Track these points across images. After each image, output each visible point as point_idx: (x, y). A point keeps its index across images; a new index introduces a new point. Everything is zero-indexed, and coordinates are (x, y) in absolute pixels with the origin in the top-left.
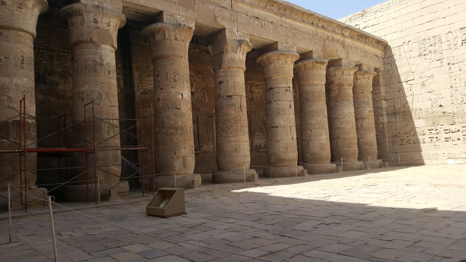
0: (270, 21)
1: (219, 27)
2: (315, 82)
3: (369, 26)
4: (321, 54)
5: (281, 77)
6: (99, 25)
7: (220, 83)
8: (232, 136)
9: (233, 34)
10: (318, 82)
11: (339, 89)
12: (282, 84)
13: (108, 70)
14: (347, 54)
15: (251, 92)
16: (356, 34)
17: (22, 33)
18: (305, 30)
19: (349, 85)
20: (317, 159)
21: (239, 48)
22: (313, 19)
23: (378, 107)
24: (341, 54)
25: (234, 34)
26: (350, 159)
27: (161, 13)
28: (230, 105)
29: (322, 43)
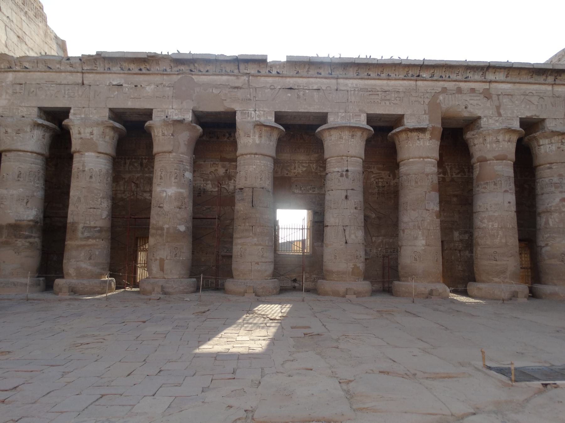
0: (315, 88)
11: (480, 166)
12: (335, 168)
13: (90, 175)
14: (498, 108)
17: (21, 153)
18: (386, 88)
26: (496, 279)
29: (427, 101)
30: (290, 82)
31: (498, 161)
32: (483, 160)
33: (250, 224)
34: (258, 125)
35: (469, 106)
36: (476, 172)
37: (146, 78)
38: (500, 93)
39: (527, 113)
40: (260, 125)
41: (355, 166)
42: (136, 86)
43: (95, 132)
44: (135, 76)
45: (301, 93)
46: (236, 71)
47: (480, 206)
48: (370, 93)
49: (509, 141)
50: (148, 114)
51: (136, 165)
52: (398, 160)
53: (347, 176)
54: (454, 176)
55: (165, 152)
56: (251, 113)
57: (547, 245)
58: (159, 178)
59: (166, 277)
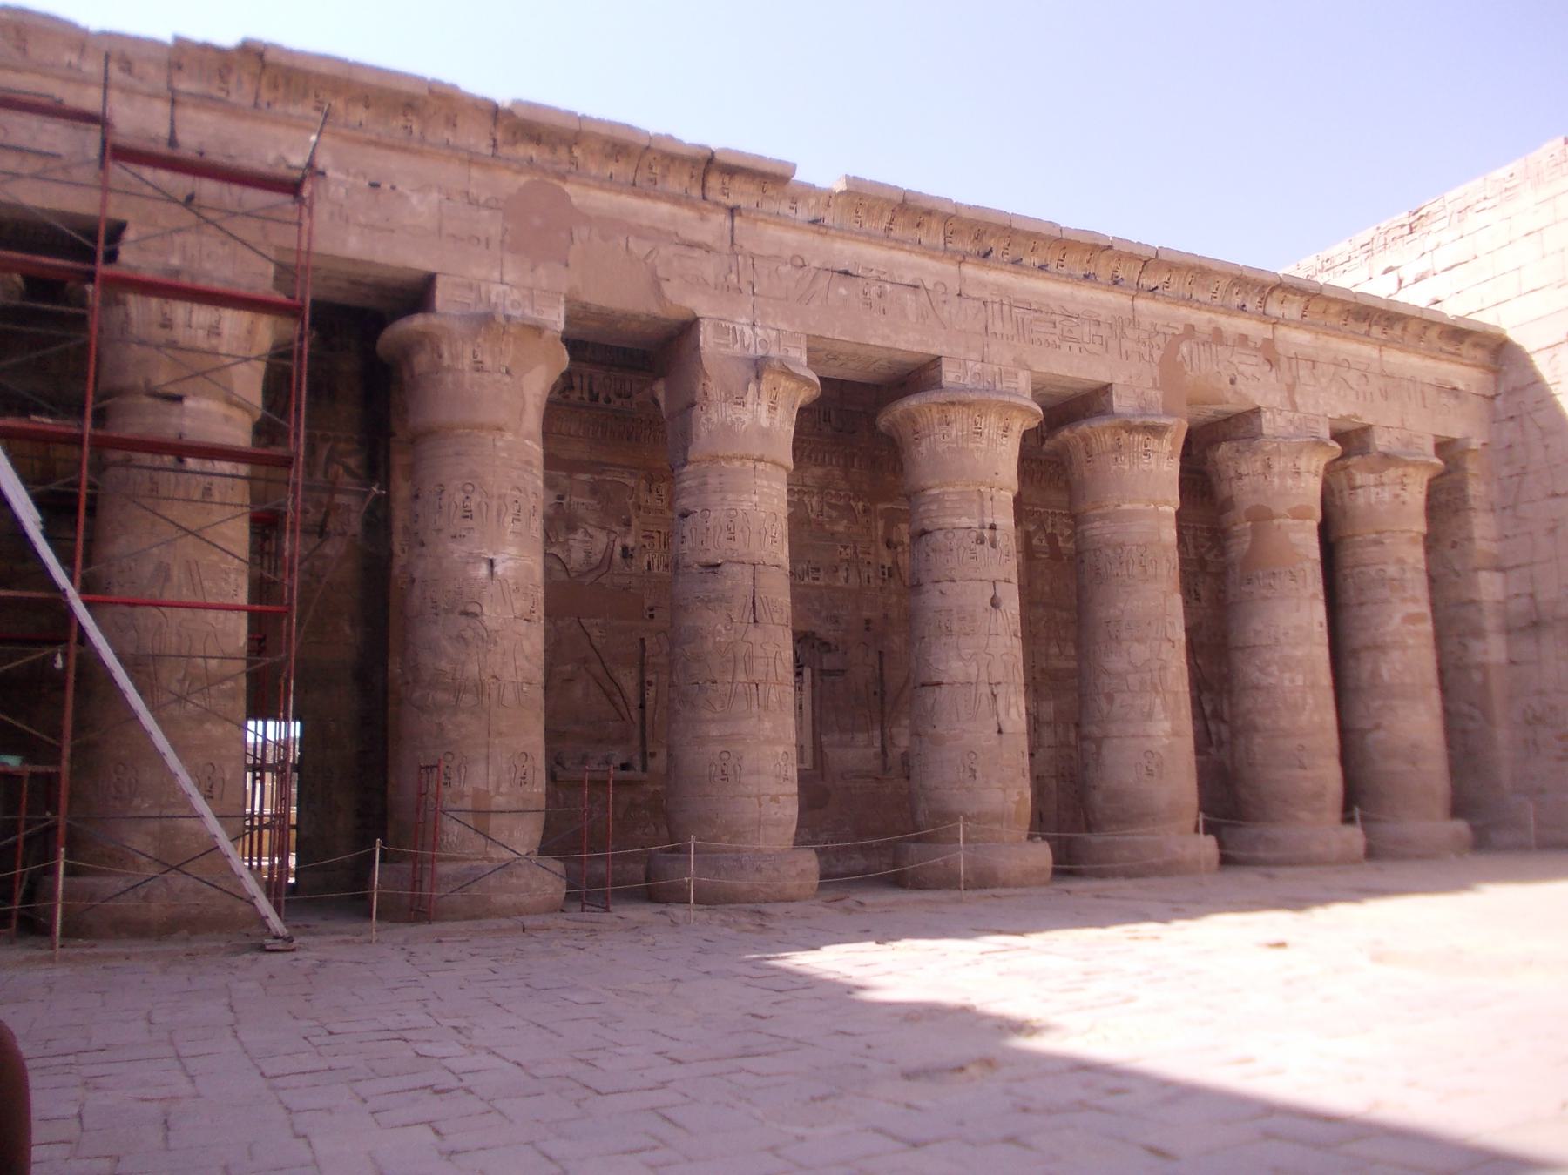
0: (907, 281)
1: (674, 315)
2: (1126, 507)
3: (1438, 269)
4: (1156, 396)
5: (958, 488)
6: (180, 334)
7: (684, 515)
8: (713, 720)
9: (730, 333)
10: (1140, 506)
12: (960, 516)
15: (889, 544)
16: (1334, 309)
18: (1071, 308)
19: (1300, 514)
20: (1134, 815)
21: (752, 386)
22: (1114, 265)
24: (1255, 388)
25: (737, 336)
27: (429, 281)
28: (710, 601)
29: (1157, 354)
30: (846, 252)
31: (1296, 522)
33: (751, 678)
35: (1239, 379)
38: (1291, 354)
42: (375, 185)
44: (372, 150)
45: (874, 290)
46: (696, 192)
47: (1257, 633)
50: (417, 294)
53: (994, 545)
56: (742, 332)
57: (1378, 727)
58: (460, 513)
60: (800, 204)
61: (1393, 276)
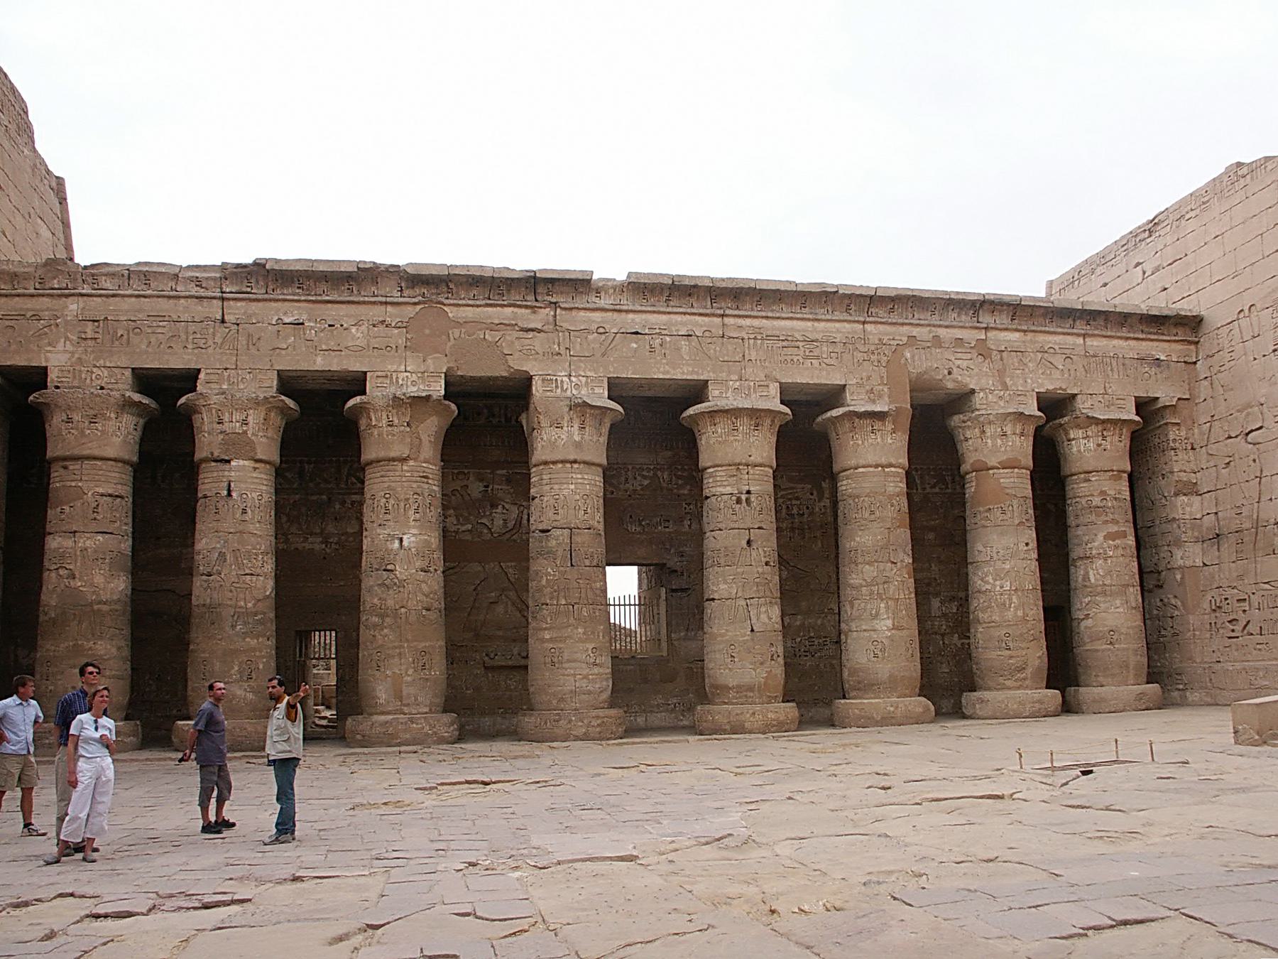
13: (243, 506)
14: (1001, 373)
23: (1170, 517)
26: (1008, 683)
30: (635, 321)
32: (982, 468)
34: (577, 405)
36: (971, 489)
37: (352, 309)
39: (1047, 385)
40: (581, 408)
41: (761, 484)
43: (250, 419)
48: (785, 344)
49: (1022, 434)
50: (357, 383)
51: (288, 475)
52: (836, 468)
54: (928, 490)
55: (394, 460)
59: (406, 709)
60: (603, 294)
61: (1139, 268)
